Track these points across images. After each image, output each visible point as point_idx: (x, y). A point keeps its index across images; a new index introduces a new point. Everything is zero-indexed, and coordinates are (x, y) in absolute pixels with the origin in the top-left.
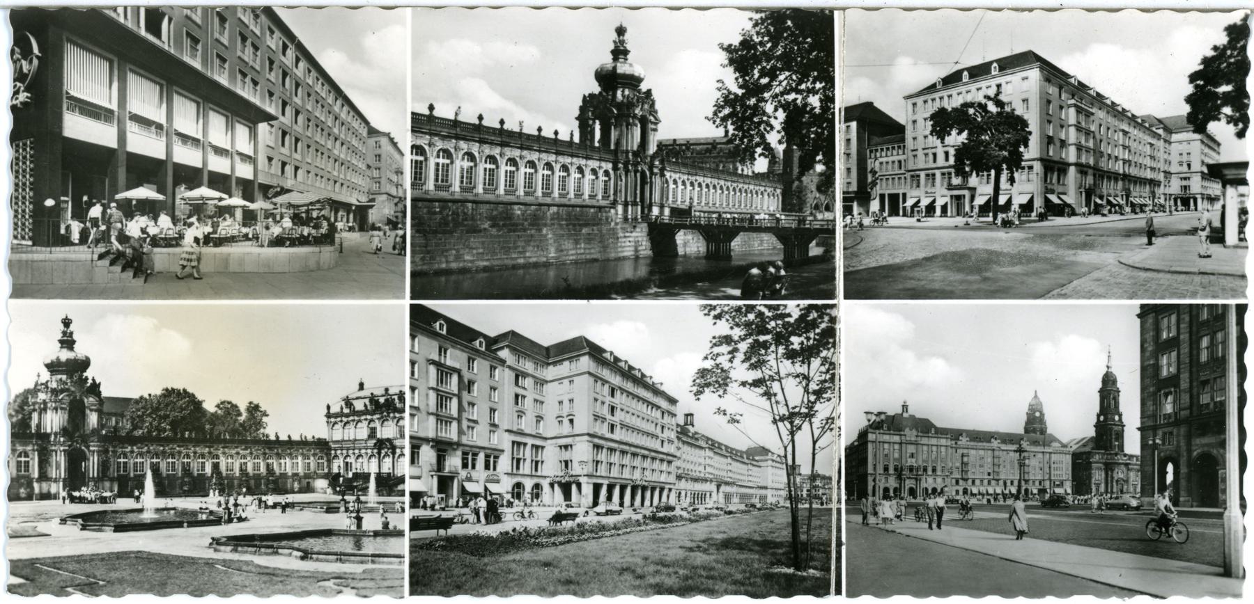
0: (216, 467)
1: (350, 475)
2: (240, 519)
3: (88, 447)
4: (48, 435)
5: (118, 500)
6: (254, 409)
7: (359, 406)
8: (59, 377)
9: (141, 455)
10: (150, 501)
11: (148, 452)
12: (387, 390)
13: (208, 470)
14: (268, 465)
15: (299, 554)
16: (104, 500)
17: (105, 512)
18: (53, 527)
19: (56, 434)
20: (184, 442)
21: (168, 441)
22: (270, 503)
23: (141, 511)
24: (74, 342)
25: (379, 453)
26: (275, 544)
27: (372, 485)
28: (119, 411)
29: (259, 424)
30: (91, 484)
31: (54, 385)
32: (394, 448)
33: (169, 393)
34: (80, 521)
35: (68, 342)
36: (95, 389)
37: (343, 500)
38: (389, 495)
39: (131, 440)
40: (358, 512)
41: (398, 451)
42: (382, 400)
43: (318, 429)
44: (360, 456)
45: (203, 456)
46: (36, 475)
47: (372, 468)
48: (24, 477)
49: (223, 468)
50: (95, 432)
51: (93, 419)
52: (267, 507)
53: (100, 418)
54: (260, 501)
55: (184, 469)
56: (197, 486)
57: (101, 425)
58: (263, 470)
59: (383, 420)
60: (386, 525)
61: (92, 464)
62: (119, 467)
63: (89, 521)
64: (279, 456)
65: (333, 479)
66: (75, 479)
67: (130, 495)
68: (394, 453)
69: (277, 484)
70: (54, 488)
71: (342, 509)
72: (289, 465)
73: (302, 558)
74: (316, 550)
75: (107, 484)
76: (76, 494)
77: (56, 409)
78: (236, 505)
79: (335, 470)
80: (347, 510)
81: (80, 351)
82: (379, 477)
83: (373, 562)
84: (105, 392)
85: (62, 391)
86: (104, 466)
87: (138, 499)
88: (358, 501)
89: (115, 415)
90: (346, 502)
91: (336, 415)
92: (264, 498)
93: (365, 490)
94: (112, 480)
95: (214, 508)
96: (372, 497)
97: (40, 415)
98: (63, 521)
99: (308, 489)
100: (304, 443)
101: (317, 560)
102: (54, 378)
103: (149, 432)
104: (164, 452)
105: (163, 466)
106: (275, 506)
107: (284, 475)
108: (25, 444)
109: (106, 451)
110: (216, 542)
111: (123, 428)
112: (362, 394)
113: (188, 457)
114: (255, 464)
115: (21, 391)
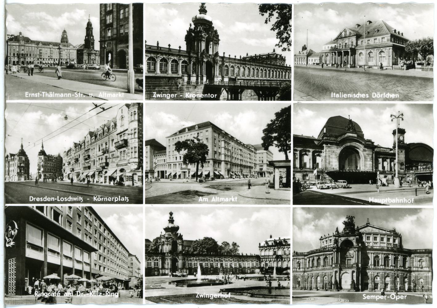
0: (222, 264)
1: (267, 268)
2: (230, 283)
3: (178, 257)
4: (165, 253)
5: (189, 276)
6: (234, 244)
7: (270, 243)
8: (168, 233)
9: (196, 260)
10: (199, 277)
11: (199, 259)
12: (280, 238)
13: (219, 266)
14: (239, 264)
15: (250, 295)
16: (184, 276)
17: (184, 280)
18: (166, 285)
19: (167, 253)
20: (211, 256)
21: (205, 255)
22: (240, 277)
23: (196, 280)
24: (174, 221)
25: (277, 260)
26: (242, 291)
27: (275, 271)
28: (189, 245)
29: (236, 250)
30: (179, 270)
31: (167, 236)
32: (282, 258)
33: (206, 239)
34: (176, 283)
35: (171, 221)
36: (181, 237)
37: (265, 276)
38: (280, 275)
39: (193, 255)
40: (270, 280)
41: (283, 259)
42: (278, 242)
43: (256, 251)
44: (270, 261)
45: (217, 261)
46: (161, 267)
47: (275, 265)
48: (156, 268)
49: (224, 265)
50: (181, 252)
51: (180, 248)
52: (239, 279)
53: (182, 248)
54: (237, 276)
55: (211, 266)
56: (215, 271)
57: (183, 250)
58: (238, 266)
59: (279, 249)
60: (279, 285)
61: (180, 263)
62: (189, 265)
63: (179, 283)
64: (243, 261)
65: (261, 269)
66: (174, 269)
67: (193, 274)
68: (282, 260)
69: (243, 271)
70: (167, 272)
71: (265, 279)
72: (247, 264)
73: (251, 296)
74: (256, 293)
75: (185, 270)
76: (174, 274)
77: (167, 244)
78: (228, 278)
79: (262, 266)
80: (266, 280)
81: (176, 224)
82: (277, 268)
83: (275, 298)
84: (185, 238)
85: (170, 238)
86: (184, 264)
87: (195, 275)
88: (270, 277)
89: (188, 246)
90: (266, 277)
91: (262, 247)
92: (238, 276)
93: (272, 273)
94: (186, 269)
95: (221, 279)
96: (275, 275)
97: (162, 246)
98: (170, 283)
99: (253, 272)
100: (251, 257)
101: (256, 297)
102: (167, 233)
103: (199, 252)
104: (204, 260)
105: (204, 264)
106: (242, 278)
107: (245, 268)
108: (157, 256)
109: (184, 259)
110: (222, 291)
111: (190, 251)
112: (271, 239)
113: (212, 261)
114: (235, 264)
115: (156, 238)
